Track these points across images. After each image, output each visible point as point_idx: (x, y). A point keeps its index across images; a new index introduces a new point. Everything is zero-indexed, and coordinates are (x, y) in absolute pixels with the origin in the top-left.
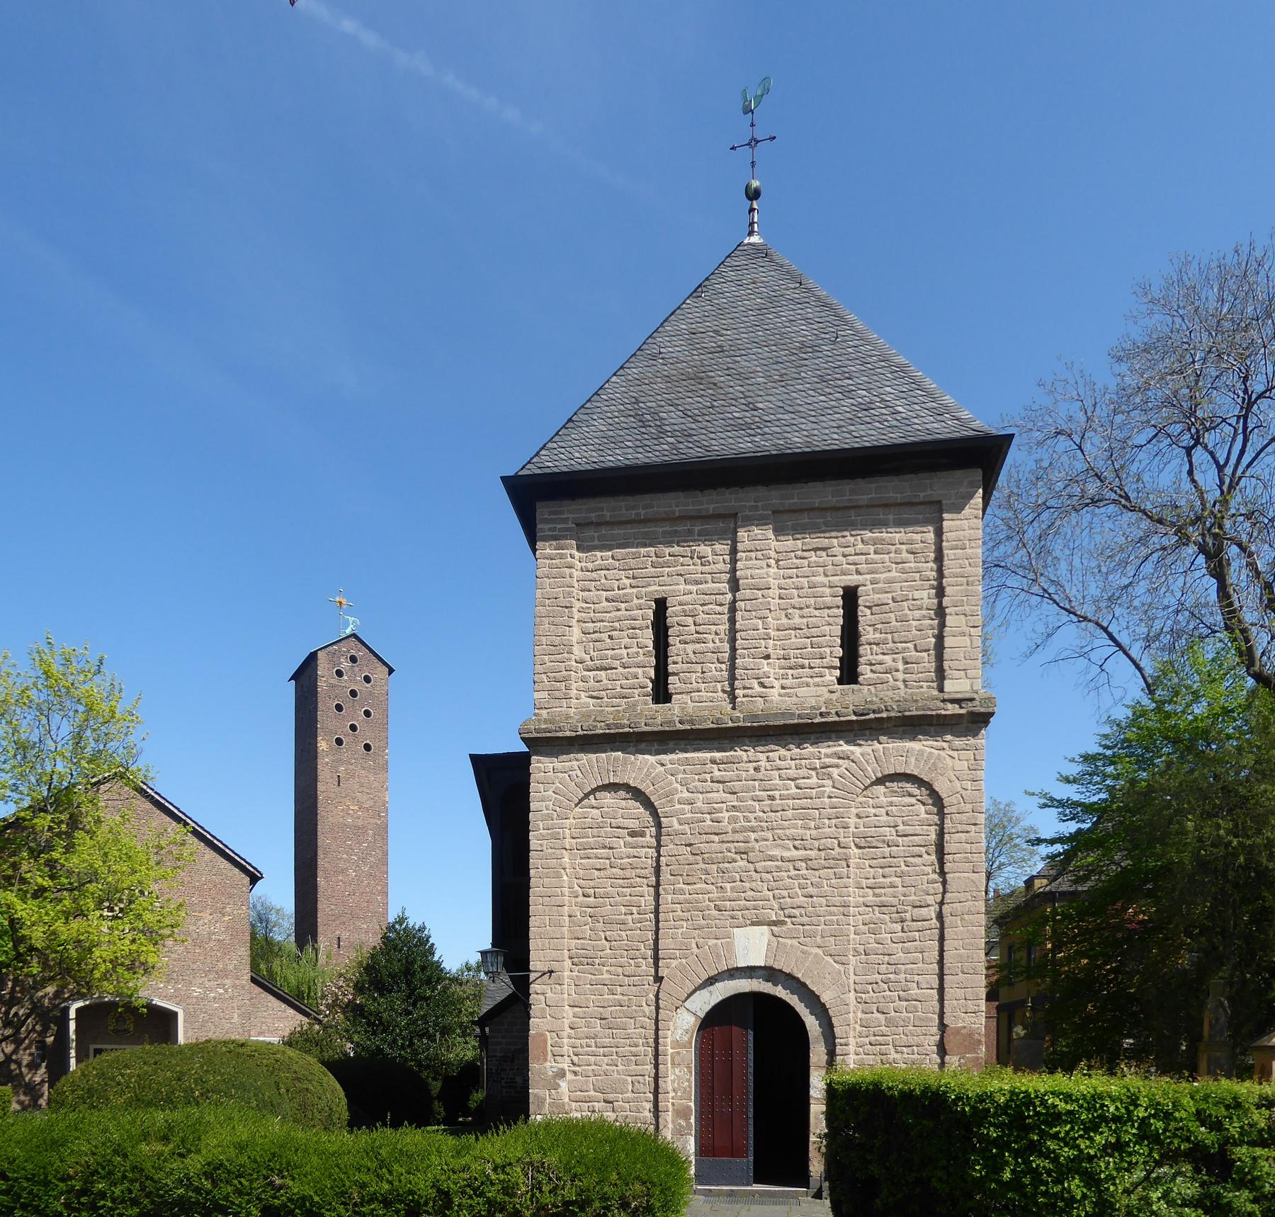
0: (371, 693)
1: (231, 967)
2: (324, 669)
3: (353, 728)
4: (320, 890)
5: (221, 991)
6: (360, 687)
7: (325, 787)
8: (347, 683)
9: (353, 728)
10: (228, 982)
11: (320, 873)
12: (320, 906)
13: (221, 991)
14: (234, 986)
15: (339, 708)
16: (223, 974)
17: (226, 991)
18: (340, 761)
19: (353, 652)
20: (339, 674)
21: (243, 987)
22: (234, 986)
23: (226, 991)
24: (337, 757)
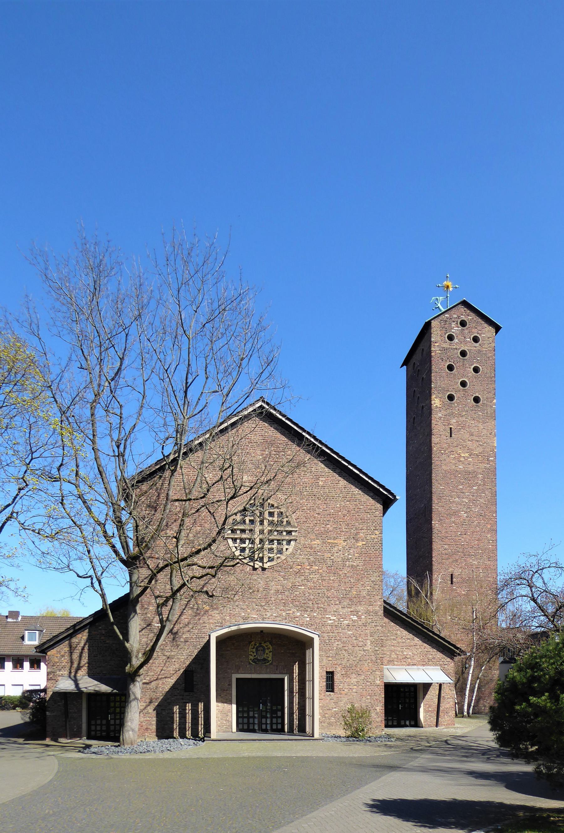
0: (479, 351)
1: (364, 593)
2: (437, 336)
3: (463, 384)
4: (435, 531)
5: (355, 618)
6: (469, 346)
7: (439, 438)
8: (458, 345)
9: (463, 384)
10: (361, 608)
11: (434, 516)
12: (435, 546)
13: (355, 618)
14: (368, 612)
15: (451, 368)
16: (357, 600)
17: (359, 617)
18: (452, 415)
19: (463, 318)
20: (451, 338)
21: (376, 613)
22: (368, 612)
23: (359, 617)
24: (448, 411)
